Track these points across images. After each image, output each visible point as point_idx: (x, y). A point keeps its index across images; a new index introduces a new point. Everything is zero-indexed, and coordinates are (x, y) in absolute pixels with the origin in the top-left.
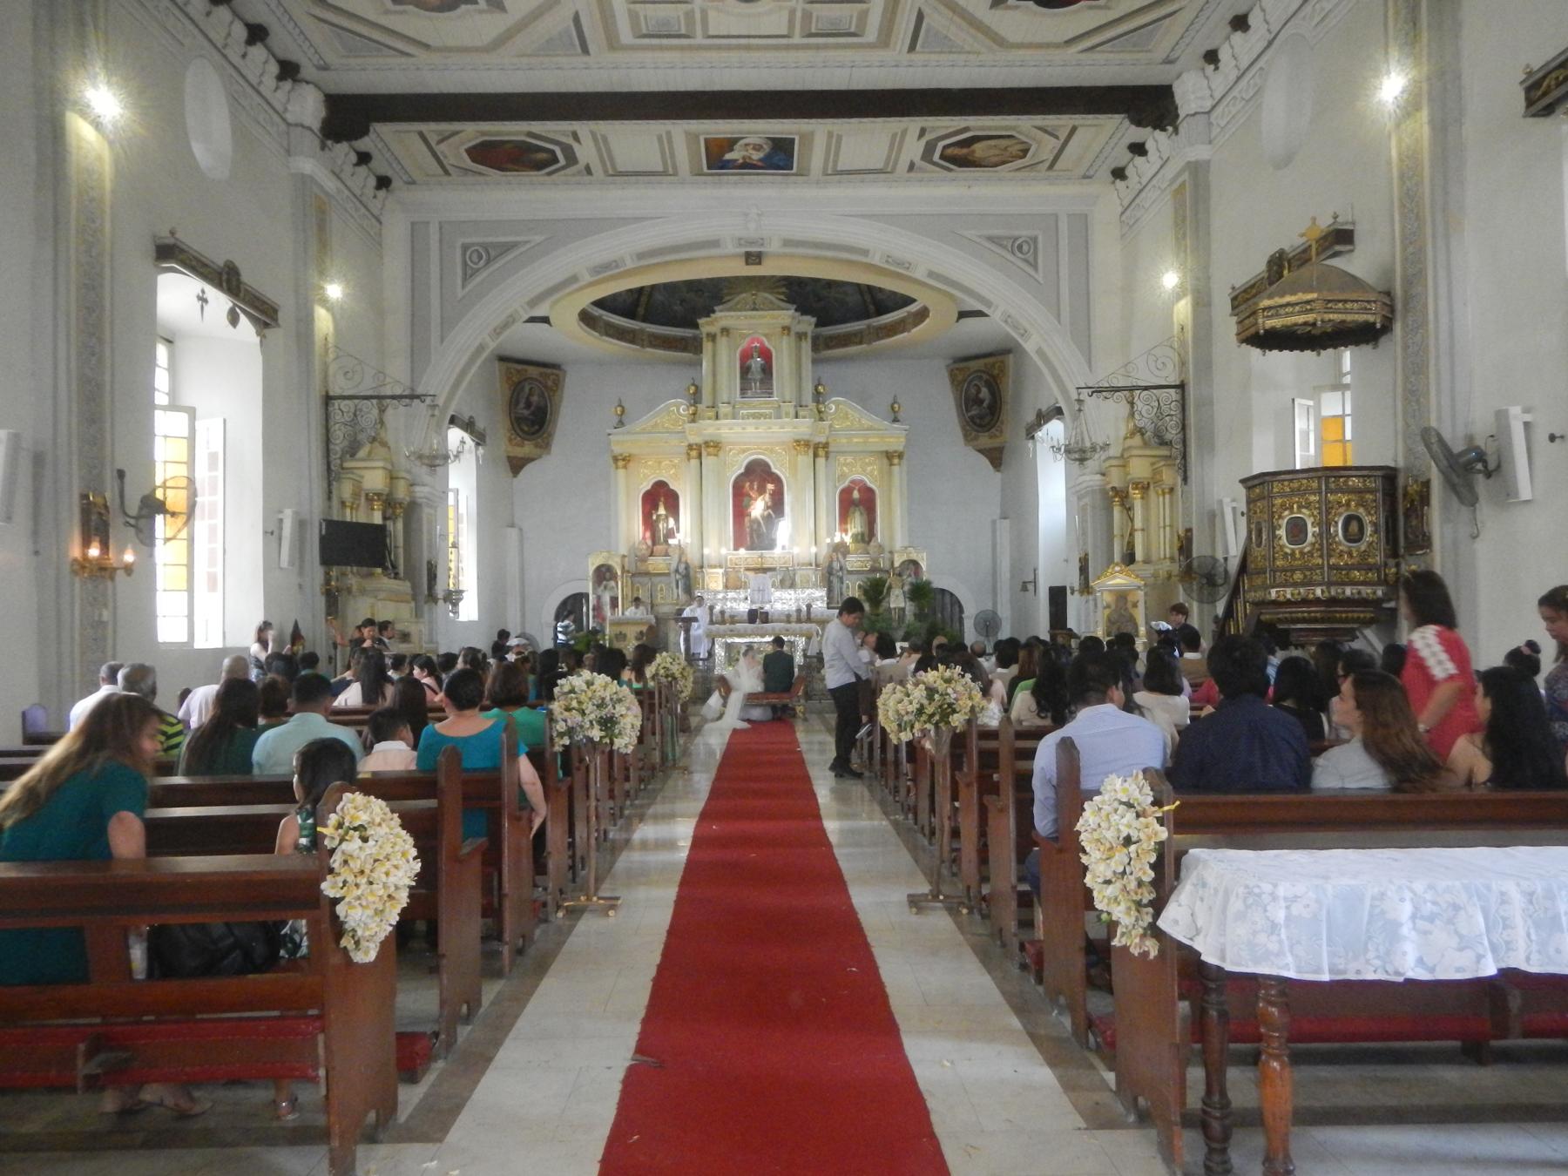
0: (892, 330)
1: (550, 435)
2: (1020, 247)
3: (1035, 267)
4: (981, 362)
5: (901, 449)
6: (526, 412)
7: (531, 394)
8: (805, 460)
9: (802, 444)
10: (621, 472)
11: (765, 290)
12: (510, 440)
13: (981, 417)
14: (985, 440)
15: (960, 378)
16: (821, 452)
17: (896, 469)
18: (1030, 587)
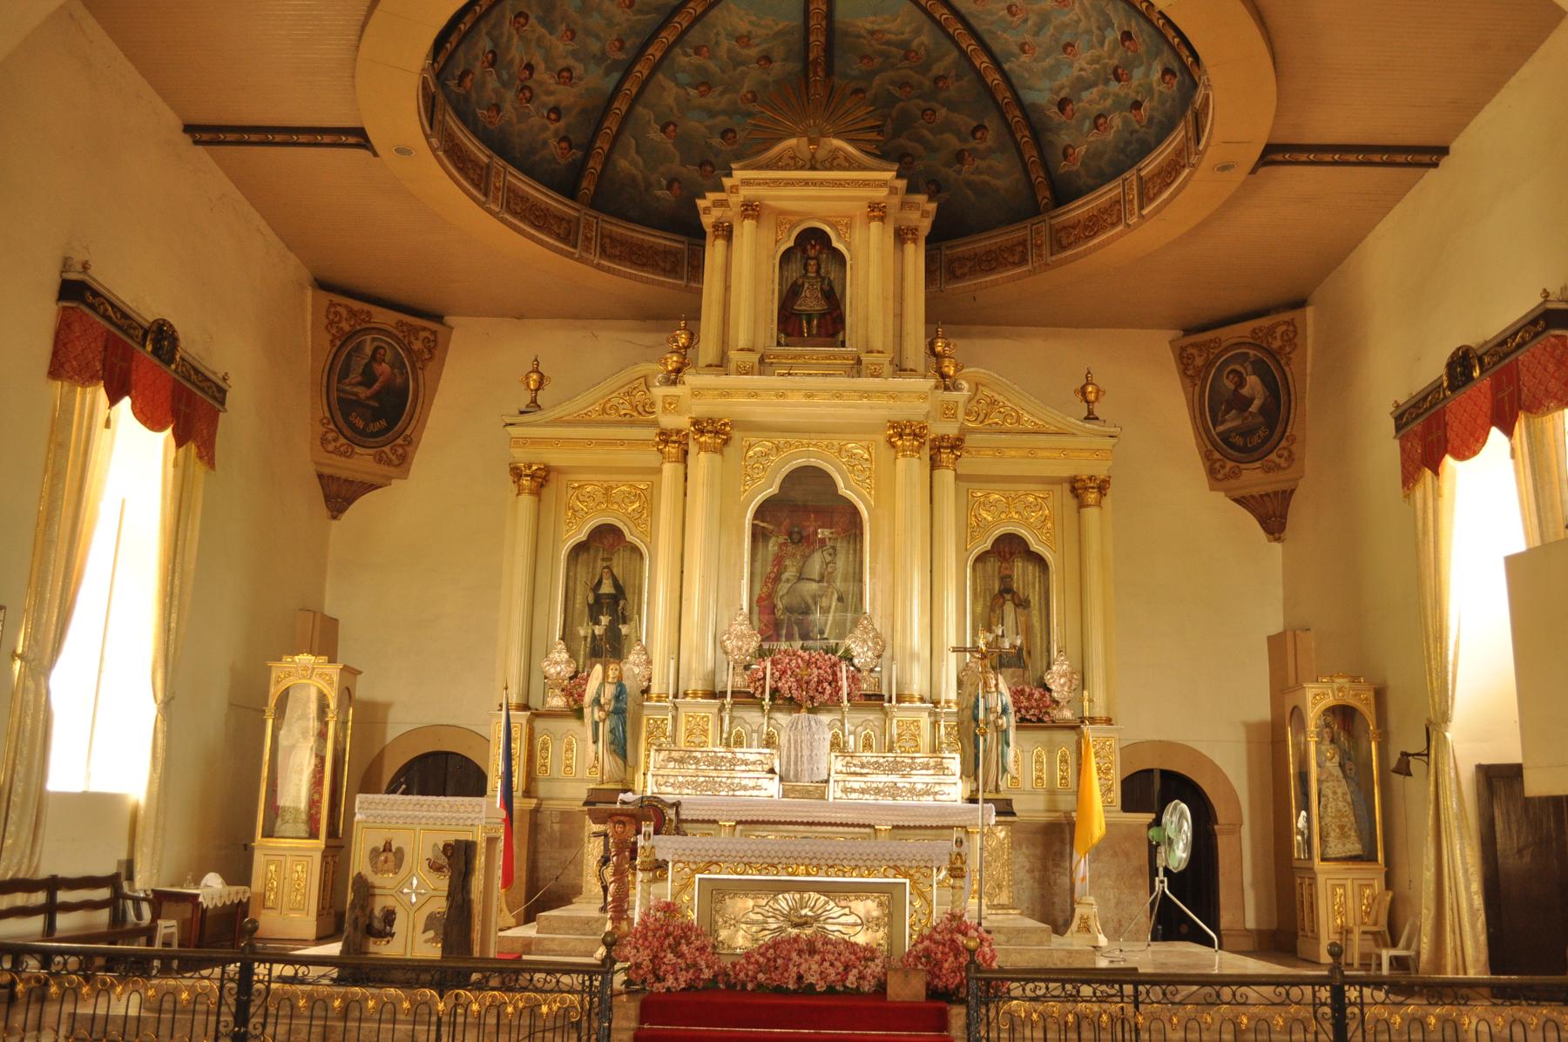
0: (1094, 225)
1: (411, 443)
4: (1244, 330)
5: (1101, 473)
6: (363, 392)
7: (373, 357)
8: (910, 469)
9: (904, 432)
10: (526, 501)
11: (837, 135)
12: (324, 441)
13: (1246, 433)
14: (1254, 478)
15: (1199, 361)
16: (945, 456)
17: (1091, 514)
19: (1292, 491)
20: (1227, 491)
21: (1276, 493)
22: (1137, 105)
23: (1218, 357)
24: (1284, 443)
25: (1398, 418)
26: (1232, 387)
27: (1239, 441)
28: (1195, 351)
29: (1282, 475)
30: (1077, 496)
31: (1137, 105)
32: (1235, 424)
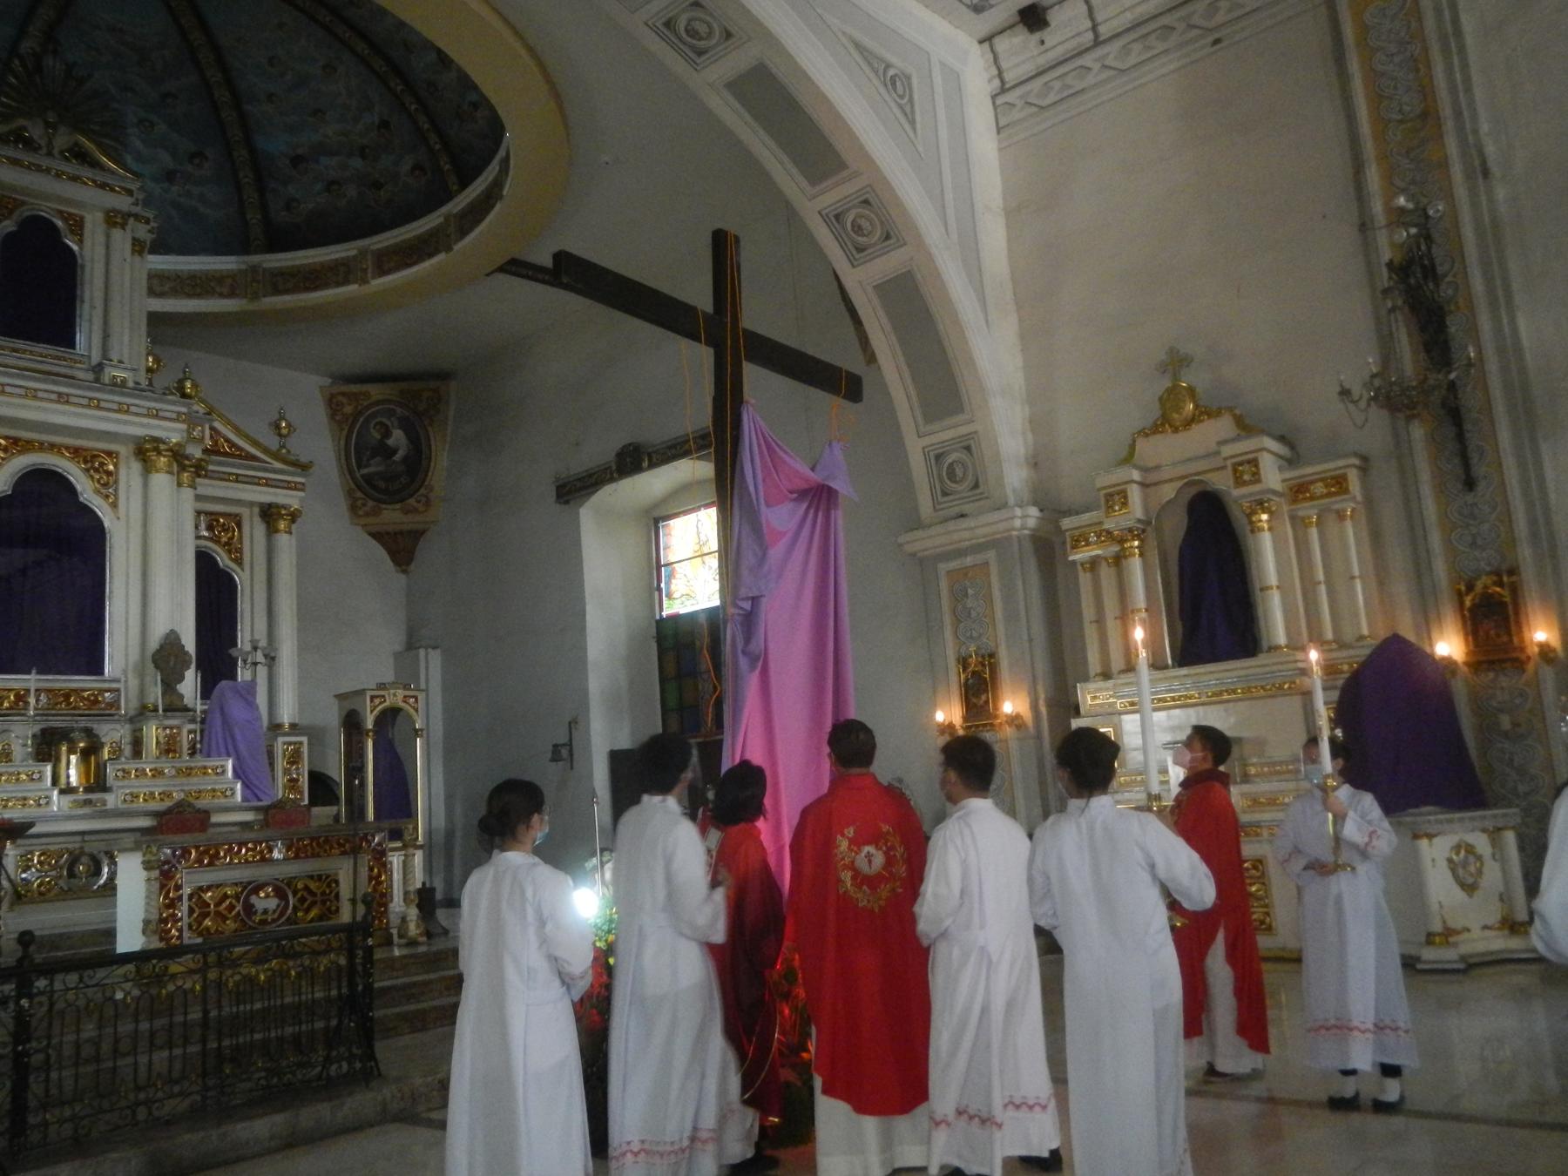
0: (313, 278)
2: (894, 84)
3: (912, 123)
14: (392, 516)
15: (348, 409)
17: (284, 541)
18: (564, 752)
19: (423, 532)
20: (364, 526)
21: (410, 532)
22: (377, 186)
23: (368, 407)
24: (422, 491)
25: (558, 488)
26: (377, 436)
27: (382, 484)
28: (345, 400)
29: (418, 518)
30: (268, 523)
31: (377, 186)
32: (381, 468)
